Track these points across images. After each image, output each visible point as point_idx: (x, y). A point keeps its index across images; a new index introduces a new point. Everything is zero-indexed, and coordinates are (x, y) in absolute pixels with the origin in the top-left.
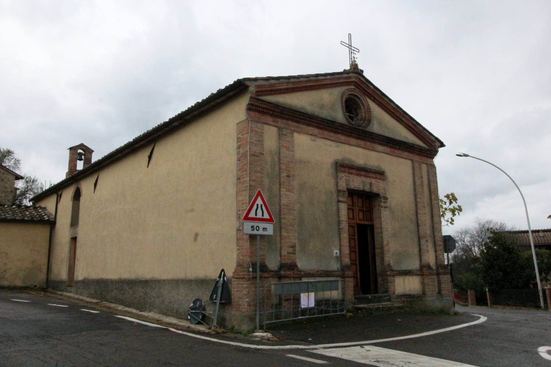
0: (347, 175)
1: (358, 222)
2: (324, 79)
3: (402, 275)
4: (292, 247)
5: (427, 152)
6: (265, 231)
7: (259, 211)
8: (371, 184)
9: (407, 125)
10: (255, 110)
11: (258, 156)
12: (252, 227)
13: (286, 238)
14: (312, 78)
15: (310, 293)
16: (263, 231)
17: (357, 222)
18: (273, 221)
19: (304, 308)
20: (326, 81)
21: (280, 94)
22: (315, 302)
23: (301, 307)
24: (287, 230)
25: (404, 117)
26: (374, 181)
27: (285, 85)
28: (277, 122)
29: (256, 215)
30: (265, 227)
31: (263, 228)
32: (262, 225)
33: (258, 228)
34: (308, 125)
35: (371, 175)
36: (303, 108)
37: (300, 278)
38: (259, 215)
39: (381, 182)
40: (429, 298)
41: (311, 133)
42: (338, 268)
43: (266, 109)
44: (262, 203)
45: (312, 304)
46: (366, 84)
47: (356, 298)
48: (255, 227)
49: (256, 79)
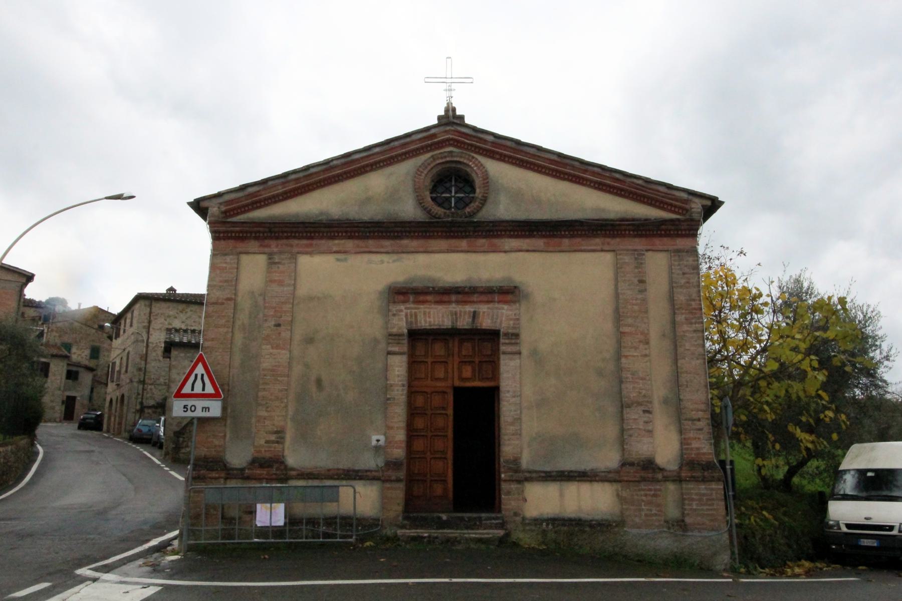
0: (412, 306)
1: (457, 383)
2: (367, 157)
4: (277, 432)
5: (663, 227)
6: (206, 411)
7: (199, 384)
8: (475, 315)
9: (600, 184)
10: (224, 239)
11: (223, 304)
12: (185, 407)
13: (265, 419)
14: (335, 162)
16: (202, 411)
17: (453, 384)
18: (220, 396)
19: (262, 527)
20: (375, 156)
21: (276, 202)
22: (285, 518)
23: (256, 525)
24: (267, 408)
25: (585, 171)
26: (483, 308)
27: (280, 187)
28: (268, 246)
29: (193, 389)
30: (206, 406)
31: (203, 408)
32: (200, 403)
33: (193, 408)
34: (333, 238)
35: (475, 298)
36: (321, 214)
37: (285, 479)
38: (198, 389)
39: (506, 307)
40: (635, 531)
41: (335, 249)
42: (377, 465)
43: (241, 232)
44: (203, 372)
45: (279, 520)
46: (474, 137)
47: (405, 518)
48: (189, 408)
49: (219, 195)
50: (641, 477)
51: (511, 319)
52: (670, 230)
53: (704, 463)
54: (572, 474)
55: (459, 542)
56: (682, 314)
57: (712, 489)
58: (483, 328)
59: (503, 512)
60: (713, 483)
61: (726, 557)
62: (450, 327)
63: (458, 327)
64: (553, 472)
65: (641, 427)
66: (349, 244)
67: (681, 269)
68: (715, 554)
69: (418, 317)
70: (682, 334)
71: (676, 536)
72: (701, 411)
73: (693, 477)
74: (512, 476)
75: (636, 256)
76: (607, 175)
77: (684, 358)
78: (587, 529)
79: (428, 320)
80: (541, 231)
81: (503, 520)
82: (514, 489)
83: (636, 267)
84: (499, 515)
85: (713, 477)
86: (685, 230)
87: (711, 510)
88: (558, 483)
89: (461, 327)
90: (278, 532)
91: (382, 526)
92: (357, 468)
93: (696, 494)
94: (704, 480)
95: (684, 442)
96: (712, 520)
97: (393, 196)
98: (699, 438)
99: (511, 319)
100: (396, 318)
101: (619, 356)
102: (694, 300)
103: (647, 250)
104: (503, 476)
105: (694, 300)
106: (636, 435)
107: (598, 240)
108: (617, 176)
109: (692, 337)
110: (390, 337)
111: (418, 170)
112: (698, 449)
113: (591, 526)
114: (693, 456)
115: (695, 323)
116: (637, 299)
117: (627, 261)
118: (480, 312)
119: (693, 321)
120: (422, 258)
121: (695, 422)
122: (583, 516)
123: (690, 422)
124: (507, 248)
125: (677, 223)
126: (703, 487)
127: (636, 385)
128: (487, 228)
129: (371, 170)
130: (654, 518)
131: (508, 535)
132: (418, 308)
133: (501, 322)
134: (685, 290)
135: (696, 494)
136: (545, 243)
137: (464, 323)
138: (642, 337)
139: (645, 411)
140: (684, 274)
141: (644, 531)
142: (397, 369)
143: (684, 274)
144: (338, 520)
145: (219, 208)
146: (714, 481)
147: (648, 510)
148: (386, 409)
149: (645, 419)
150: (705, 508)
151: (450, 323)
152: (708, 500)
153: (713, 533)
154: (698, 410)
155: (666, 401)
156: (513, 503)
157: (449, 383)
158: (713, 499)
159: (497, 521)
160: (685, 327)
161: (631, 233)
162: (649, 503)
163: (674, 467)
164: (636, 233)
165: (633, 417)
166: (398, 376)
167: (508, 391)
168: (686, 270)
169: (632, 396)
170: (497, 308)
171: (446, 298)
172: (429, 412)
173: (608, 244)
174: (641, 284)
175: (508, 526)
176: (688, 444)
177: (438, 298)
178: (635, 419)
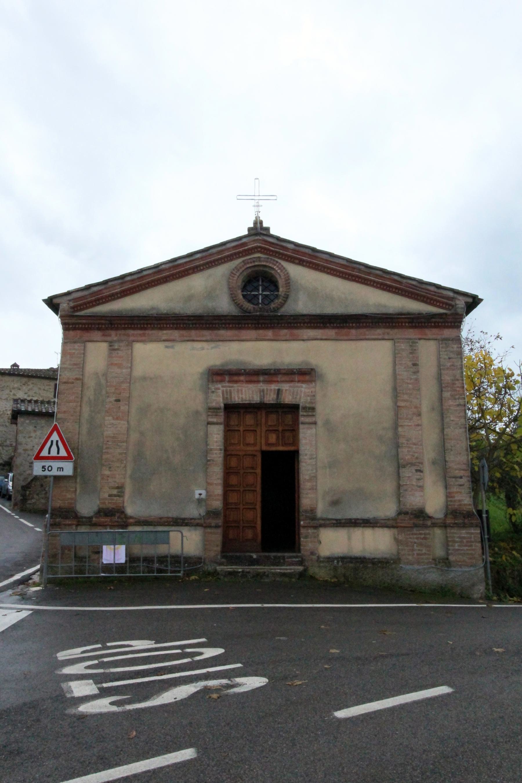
0: (227, 384)
1: (264, 448)
3: (343, 526)
4: (118, 488)
5: (434, 320)
6: (60, 471)
7: (54, 447)
8: (279, 392)
9: (382, 284)
10: (74, 329)
11: (73, 383)
12: (43, 467)
13: (108, 477)
14: (163, 266)
15: (116, 546)
16: (58, 471)
18: (72, 458)
19: (107, 564)
20: (196, 261)
21: (114, 299)
22: (126, 556)
23: (102, 562)
24: (110, 468)
25: (369, 274)
26: (285, 387)
27: (118, 287)
28: (110, 335)
29: (49, 453)
31: (58, 468)
32: (55, 464)
33: (50, 469)
34: (161, 329)
35: (279, 378)
36: (153, 308)
37: (125, 526)
38: (54, 453)
39: (304, 386)
40: (408, 567)
41: (164, 338)
42: (200, 514)
43: (88, 324)
44: (58, 439)
45: (121, 559)
47: (223, 557)
48: (46, 468)
49: (69, 293)
50: (414, 523)
51: (308, 396)
52: (438, 323)
53: (465, 512)
54: (358, 521)
55: (268, 576)
56: (448, 391)
57: (472, 534)
58: (286, 402)
59: (302, 552)
60: (472, 528)
61: (481, 588)
62: (259, 402)
63: (265, 402)
64: (342, 519)
65: (414, 483)
66: (176, 334)
67: (447, 355)
68: (473, 585)
69: (233, 394)
70: (448, 407)
71: (442, 571)
72: (464, 470)
73: (455, 523)
74: (309, 523)
75: (411, 344)
76: (388, 277)
77: (449, 427)
78: (370, 565)
79: (240, 396)
80: (333, 323)
81: (302, 558)
82: (311, 533)
83: (411, 353)
84: (299, 555)
85: (472, 523)
86: (451, 322)
87: (470, 550)
88: (347, 528)
89: (267, 402)
90: (120, 568)
91: (204, 563)
92: (183, 516)
93: (459, 537)
94: (464, 526)
95: (448, 495)
96: (471, 558)
97: (210, 294)
98: (461, 493)
99: (308, 396)
100: (214, 395)
101: (396, 426)
102: (458, 380)
103: (420, 339)
104: (302, 523)
105: (458, 380)
106: (410, 489)
107: (379, 331)
108: (396, 278)
109: (456, 410)
110: (210, 411)
111: (232, 273)
112: (460, 501)
113: (373, 563)
114: (456, 506)
115: (459, 398)
116: (411, 379)
117: (403, 348)
118: (283, 390)
119: (457, 397)
120: (235, 346)
121: (458, 479)
122: (367, 555)
123: (454, 479)
124: (305, 337)
125: (444, 316)
126: (464, 531)
127: (410, 449)
128: (289, 321)
129: (194, 272)
130: (424, 557)
131: (305, 570)
132: (232, 387)
133: (300, 398)
134: (450, 372)
135: (459, 537)
136: (336, 333)
137: (270, 398)
138: (415, 410)
139: (417, 471)
140: (449, 358)
141: (416, 567)
142: (215, 436)
143: (449, 358)
144: (169, 559)
145: (68, 304)
146: (472, 527)
147: (419, 550)
148: (207, 468)
149: (418, 477)
150: (465, 548)
151: (259, 399)
152: (467, 542)
153: (472, 569)
154: (460, 470)
155: (434, 463)
156: (310, 545)
157: (258, 448)
158: (471, 542)
159: (297, 560)
160: (451, 402)
161: (407, 324)
162: (421, 544)
163: (440, 515)
164: (410, 325)
165: (407, 475)
166: (216, 442)
167: (306, 455)
168: (452, 355)
169: (407, 458)
170: (297, 387)
171: (255, 378)
172: (242, 472)
173: (388, 334)
174: (414, 367)
175: (306, 563)
176: (452, 497)
177: (248, 378)
178: (409, 477)
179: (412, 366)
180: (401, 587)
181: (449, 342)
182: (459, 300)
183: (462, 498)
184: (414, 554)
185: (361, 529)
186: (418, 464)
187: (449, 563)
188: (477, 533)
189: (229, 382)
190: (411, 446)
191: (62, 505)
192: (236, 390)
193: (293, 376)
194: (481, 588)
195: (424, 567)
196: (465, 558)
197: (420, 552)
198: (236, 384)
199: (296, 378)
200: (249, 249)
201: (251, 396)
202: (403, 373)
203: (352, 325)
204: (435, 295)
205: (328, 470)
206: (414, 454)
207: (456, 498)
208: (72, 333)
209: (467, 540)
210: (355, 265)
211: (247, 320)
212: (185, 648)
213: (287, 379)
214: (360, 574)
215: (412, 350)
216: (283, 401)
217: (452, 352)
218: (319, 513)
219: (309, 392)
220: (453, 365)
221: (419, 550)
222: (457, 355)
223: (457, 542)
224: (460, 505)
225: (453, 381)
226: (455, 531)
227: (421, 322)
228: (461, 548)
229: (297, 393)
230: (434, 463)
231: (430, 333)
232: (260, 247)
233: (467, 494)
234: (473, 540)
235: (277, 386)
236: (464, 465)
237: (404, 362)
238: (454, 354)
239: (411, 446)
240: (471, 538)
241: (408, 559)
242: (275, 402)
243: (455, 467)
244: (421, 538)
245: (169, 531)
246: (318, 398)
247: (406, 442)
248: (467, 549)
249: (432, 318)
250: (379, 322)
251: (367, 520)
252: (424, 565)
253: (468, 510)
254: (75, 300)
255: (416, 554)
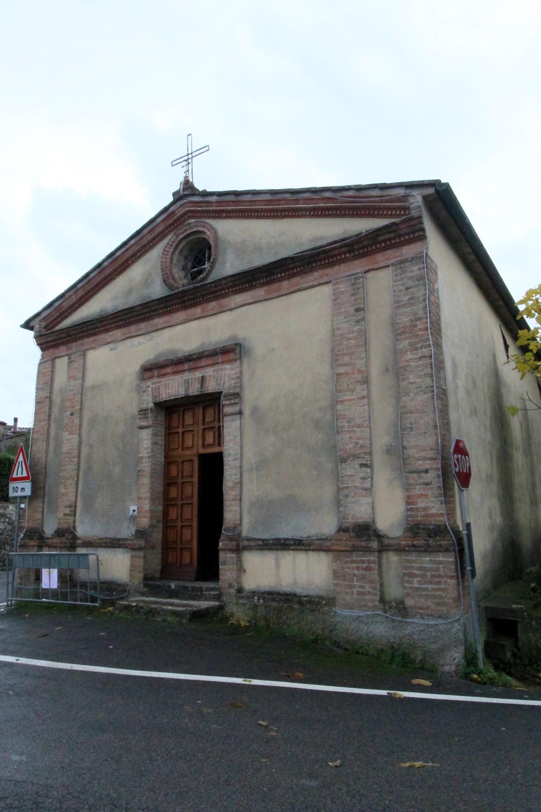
1: (202, 451)
2: (127, 250)
3: (271, 549)
4: (70, 506)
5: (381, 238)
8: (203, 379)
9: (314, 209)
15: (51, 570)
17: (198, 451)
25: (297, 201)
26: (209, 372)
30: (23, 487)
31: (22, 488)
35: (203, 362)
39: (228, 366)
40: (346, 612)
44: (23, 460)
47: (146, 585)
50: (354, 546)
51: (233, 379)
52: (390, 239)
53: (432, 527)
54: (288, 542)
55: (159, 614)
56: (406, 339)
57: (440, 562)
58: (210, 391)
59: (220, 583)
60: (440, 554)
61: (456, 655)
62: (184, 396)
63: (190, 395)
64: (270, 539)
65: (357, 485)
66: (118, 333)
67: (403, 284)
68: (442, 650)
69: (161, 390)
70: (406, 364)
71: (393, 621)
72: (430, 459)
73: (414, 546)
74: (227, 545)
75: (353, 282)
76: (318, 197)
77: (407, 394)
78: (296, 606)
79: (168, 391)
80: (259, 279)
81: (220, 592)
82: (229, 558)
83: (353, 295)
84: (217, 586)
85: (441, 546)
86: (408, 234)
87: (437, 590)
88: (275, 552)
89: (192, 395)
90: (53, 593)
91: (129, 593)
92: (119, 537)
93: (419, 569)
94: (427, 550)
95: (409, 501)
96: (438, 604)
97: (147, 282)
98: (426, 496)
99: (233, 379)
100: (145, 394)
101: (335, 403)
102: (420, 319)
103: (366, 272)
104: (220, 544)
105: (420, 319)
106: (353, 494)
107: (316, 274)
108: (328, 194)
109: (418, 366)
110: (141, 413)
111: (164, 250)
112: (425, 509)
113: (300, 603)
114: (419, 518)
115: (421, 348)
116: (353, 332)
117: (343, 289)
118: (207, 376)
119: (419, 345)
120: (166, 333)
121: (422, 475)
122: (298, 591)
123: (415, 475)
124: (232, 306)
125: (394, 228)
126: (428, 559)
127: (352, 435)
128: (212, 290)
129: (133, 262)
130: (368, 597)
131: (221, 608)
132: (161, 382)
133: (224, 382)
134: (409, 309)
135: (419, 569)
136: (265, 291)
137: (194, 390)
138: (359, 377)
139: (362, 465)
140: (407, 289)
141: (356, 613)
142: (145, 442)
143: (407, 289)
144: (88, 585)
145: (40, 324)
146: (440, 551)
147: (361, 587)
148: (138, 480)
149: (362, 475)
150: (430, 586)
151: (184, 393)
152: (433, 576)
153: (441, 621)
154: (426, 459)
155: (389, 451)
156: (228, 574)
157: (194, 452)
158: (440, 576)
159: (215, 593)
160: (409, 356)
161: (348, 255)
162: (362, 578)
163: (397, 533)
164: (352, 254)
165: (349, 474)
166: (146, 449)
167: (230, 455)
168: (410, 283)
169: (348, 448)
170: (221, 370)
171: (180, 368)
172: (180, 481)
173: (327, 275)
174: (358, 313)
175: (224, 598)
176: (412, 503)
177: (175, 369)
178: (351, 476)
179: (354, 312)
180: (336, 641)
181: (407, 264)
182: (413, 196)
183: (428, 505)
184: (353, 593)
185: (291, 552)
186: (362, 455)
187: (405, 608)
188: (450, 562)
189: (159, 376)
190: (355, 429)
191: (33, 525)
192: (164, 385)
193: (216, 357)
194: (456, 655)
195: (368, 613)
196: (429, 603)
197: (362, 589)
198: (164, 378)
199: (220, 359)
200: (179, 218)
201: (177, 390)
202: (342, 325)
203: (281, 275)
204: (381, 202)
205: (255, 472)
206: (358, 441)
207: (420, 505)
208: (47, 352)
209: (433, 573)
210: (280, 196)
211: (171, 300)
212: (528, 692)
213: (211, 363)
214: (284, 618)
215: (354, 290)
216: (207, 390)
217: (409, 278)
218: (246, 531)
219: (233, 374)
220: (412, 298)
221: (361, 587)
222: (418, 280)
223: (415, 576)
224: (427, 515)
225: (412, 322)
226: (414, 558)
227: (367, 247)
228: (423, 586)
229: (221, 377)
230: (389, 451)
231: (381, 258)
232: (189, 211)
233: (436, 497)
234: (441, 573)
235: (201, 373)
236: (429, 452)
237: (343, 310)
238: (414, 280)
239: (355, 429)
240: (438, 569)
241: (344, 600)
242: (199, 393)
243: (417, 456)
244: (363, 569)
245: (88, 554)
246: (245, 380)
247: (347, 424)
248: (433, 589)
249: (378, 236)
250: (311, 263)
251: (299, 540)
252: (368, 611)
253: (438, 523)
254: (44, 319)
255: (355, 593)
